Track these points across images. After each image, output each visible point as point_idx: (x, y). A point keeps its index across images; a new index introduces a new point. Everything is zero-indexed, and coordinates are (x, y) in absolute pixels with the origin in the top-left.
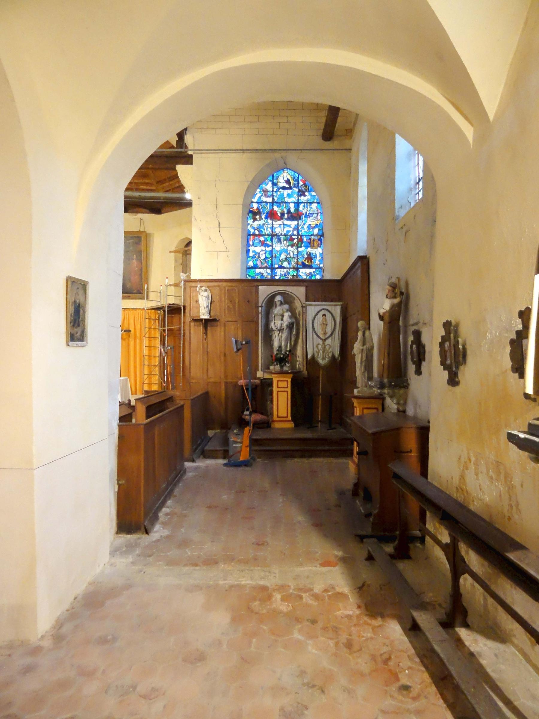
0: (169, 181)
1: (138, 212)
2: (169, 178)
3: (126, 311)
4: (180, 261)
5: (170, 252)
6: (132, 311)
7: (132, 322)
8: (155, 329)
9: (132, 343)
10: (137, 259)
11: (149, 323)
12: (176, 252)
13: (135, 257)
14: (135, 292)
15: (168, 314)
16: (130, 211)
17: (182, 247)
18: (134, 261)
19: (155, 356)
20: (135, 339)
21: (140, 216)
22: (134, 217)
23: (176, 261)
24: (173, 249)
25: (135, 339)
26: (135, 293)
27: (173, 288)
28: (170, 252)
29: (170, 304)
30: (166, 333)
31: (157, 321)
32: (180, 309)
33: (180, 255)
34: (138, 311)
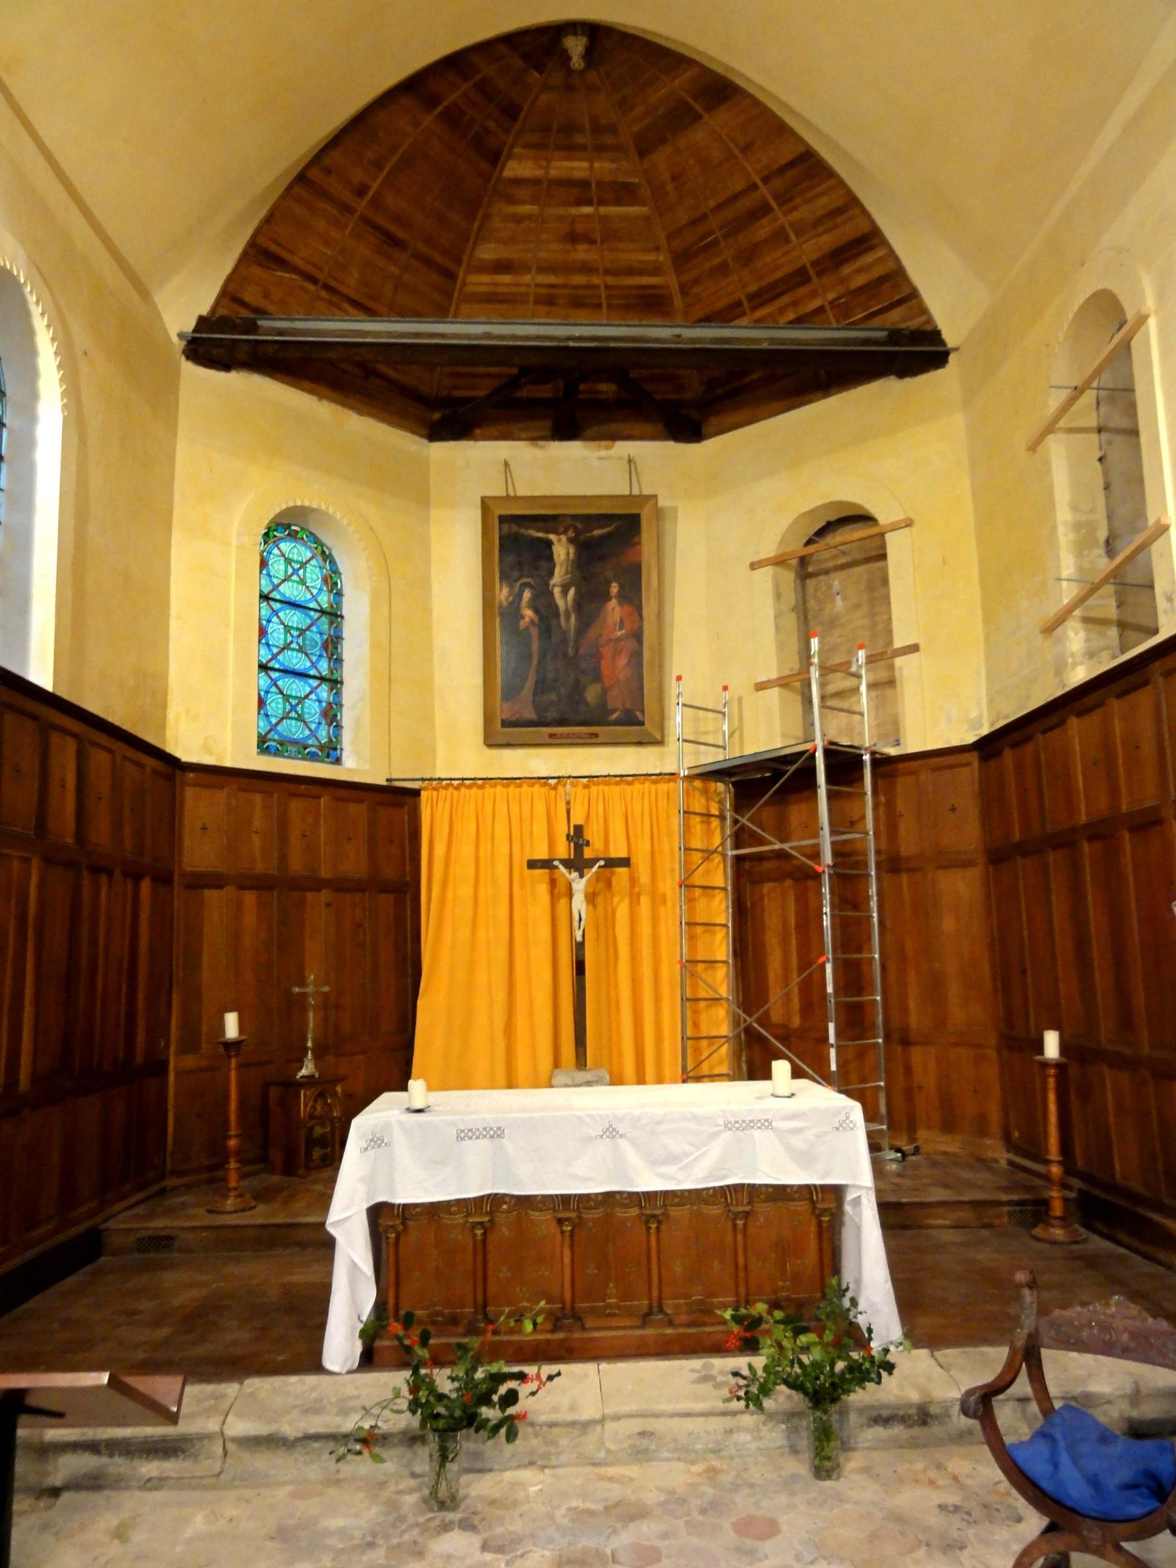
0: (754, 309)
1: (615, 437)
2: (751, 297)
3: (594, 789)
4: (790, 597)
5: (754, 566)
6: (617, 789)
7: (617, 827)
8: (708, 854)
9: (622, 911)
10: (623, 597)
11: (687, 829)
12: (779, 562)
13: (615, 588)
14: (614, 716)
15: (829, 780)
16: (588, 432)
17: (796, 546)
18: (613, 603)
19: (711, 963)
20: (635, 899)
21: (624, 448)
22: (603, 453)
23: (778, 596)
24: (769, 549)
25: (635, 899)
26: (609, 724)
27: (775, 692)
28: (754, 566)
29: (831, 743)
30: (828, 857)
31: (715, 823)
32: (857, 761)
33: (789, 577)
34: (638, 787)
